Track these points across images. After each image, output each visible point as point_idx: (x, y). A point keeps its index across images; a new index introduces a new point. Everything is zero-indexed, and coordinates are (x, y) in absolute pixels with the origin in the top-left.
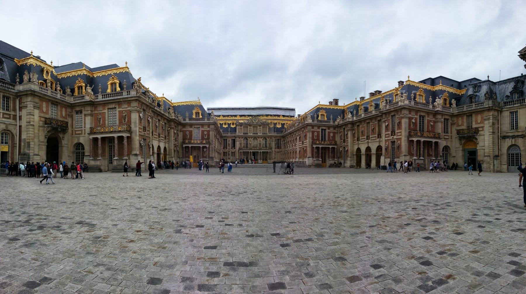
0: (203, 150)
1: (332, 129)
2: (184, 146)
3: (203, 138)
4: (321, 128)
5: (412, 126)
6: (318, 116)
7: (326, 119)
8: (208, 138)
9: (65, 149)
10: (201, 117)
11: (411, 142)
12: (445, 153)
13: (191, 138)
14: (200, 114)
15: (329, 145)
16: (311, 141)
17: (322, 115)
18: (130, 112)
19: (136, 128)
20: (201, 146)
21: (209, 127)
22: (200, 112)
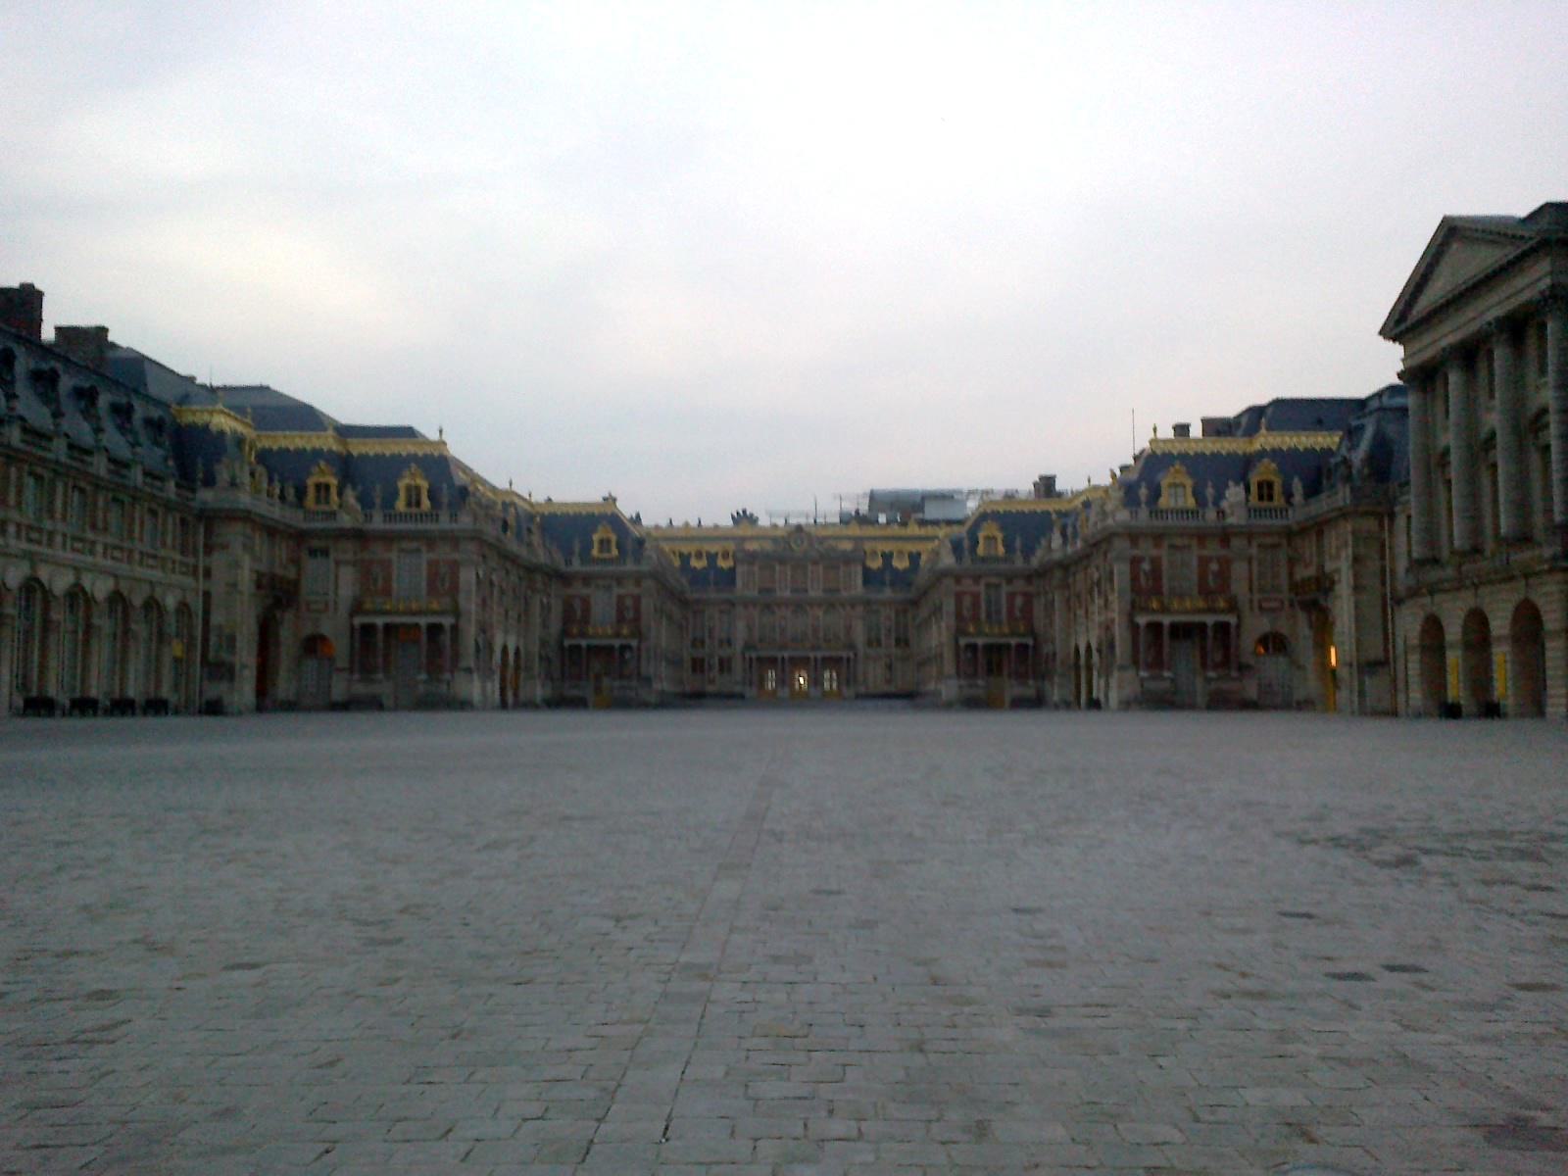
0: (622, 655)
1: (1020, 585)
2: (567, 643)
3: (621, 619)
6: (975, 543)
7: (1001, 550)
8: (637, 619)
9: (283, 650)
10: (615, 552)
11: (1134, 628)
14: (614, 544)
15: (1005, 635)
16: (952, 621)
18: (455, 566)
19: (470, 604)
20: (617, 643)
21: (638, 583)
22: (614, 538)
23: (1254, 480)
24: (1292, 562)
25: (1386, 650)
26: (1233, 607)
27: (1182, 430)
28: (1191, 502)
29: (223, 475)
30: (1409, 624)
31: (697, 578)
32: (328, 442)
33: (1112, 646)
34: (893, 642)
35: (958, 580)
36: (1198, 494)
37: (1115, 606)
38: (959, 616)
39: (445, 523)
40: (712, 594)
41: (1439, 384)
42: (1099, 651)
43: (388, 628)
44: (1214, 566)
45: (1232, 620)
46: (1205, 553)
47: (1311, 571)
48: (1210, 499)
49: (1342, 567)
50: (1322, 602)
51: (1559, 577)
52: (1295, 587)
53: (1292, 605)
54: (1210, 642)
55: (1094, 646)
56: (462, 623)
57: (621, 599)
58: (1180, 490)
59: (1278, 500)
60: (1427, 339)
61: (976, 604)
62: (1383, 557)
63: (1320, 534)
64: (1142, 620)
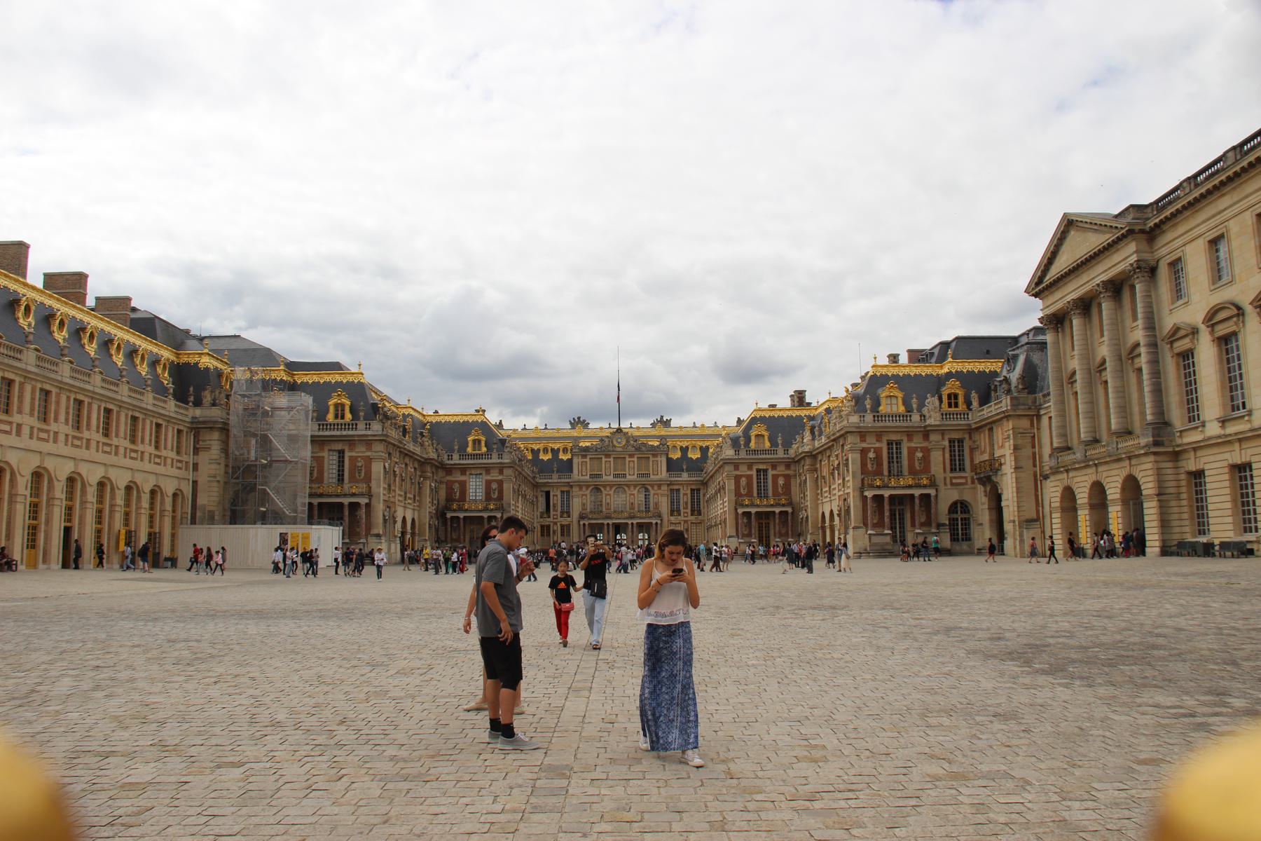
1: (781, 469)
3: (488, 498)
4: (755, 467)
5: (869, 466)
6: (748, 440)
7: (767, 444)
8: (500, 498)
10: (484, 449)
11: (864, 498)
12: (959, 516)
13: (463, 497)
15: (772, 506)
16: (733, 498)
17: (757, 436)
18: (369, 461)
20: (485, 515)
21: (501, 472)
22: (483, 439)
23: (945, 392)
24: (972, 450)
25: (1038, 512)
26: (933, 484)
27: (894, 358)
28: (902, 409)
29: (207, 397)
30: (1052, 492)
31: (545, 468)
32: (281, 375)
33: (848, 511)
34: (689, 511)
35: (736, 467)
36: (906, 403)
37: (850, 484)
38: (738, 493)
39: (361, 430)
40: (555, 478)
41: (1067, 324)
42: (839, 515)
43: (320, 504)
44: (919, 455)
45: (932, 492)
46: (913, 445)
47: (986, 457)
48: (915, 406)
49: (1006, 452)
50: (994, 478)
51: (1152, 458)
52: (974, 468)
53: (973, 482)
54: (917, 508)
55: (836, 512)
56: (374, 502)
57: (488, 483)
58: (894, 401)
59: (962, 406)
60: (1058, 295)
61: (749, 485)
62: (1034, 447)
63: (991, 430)
64: (869, 494)
